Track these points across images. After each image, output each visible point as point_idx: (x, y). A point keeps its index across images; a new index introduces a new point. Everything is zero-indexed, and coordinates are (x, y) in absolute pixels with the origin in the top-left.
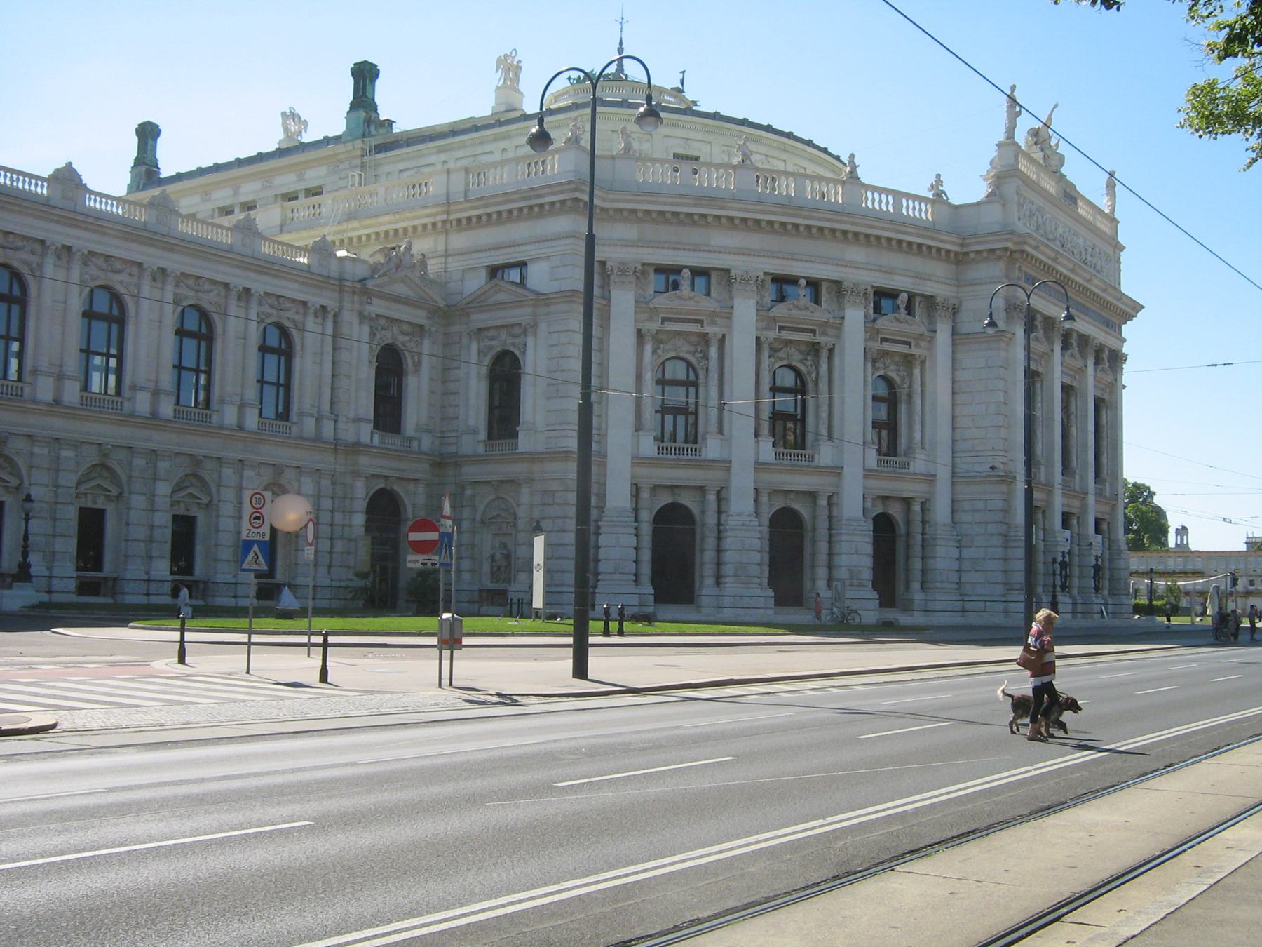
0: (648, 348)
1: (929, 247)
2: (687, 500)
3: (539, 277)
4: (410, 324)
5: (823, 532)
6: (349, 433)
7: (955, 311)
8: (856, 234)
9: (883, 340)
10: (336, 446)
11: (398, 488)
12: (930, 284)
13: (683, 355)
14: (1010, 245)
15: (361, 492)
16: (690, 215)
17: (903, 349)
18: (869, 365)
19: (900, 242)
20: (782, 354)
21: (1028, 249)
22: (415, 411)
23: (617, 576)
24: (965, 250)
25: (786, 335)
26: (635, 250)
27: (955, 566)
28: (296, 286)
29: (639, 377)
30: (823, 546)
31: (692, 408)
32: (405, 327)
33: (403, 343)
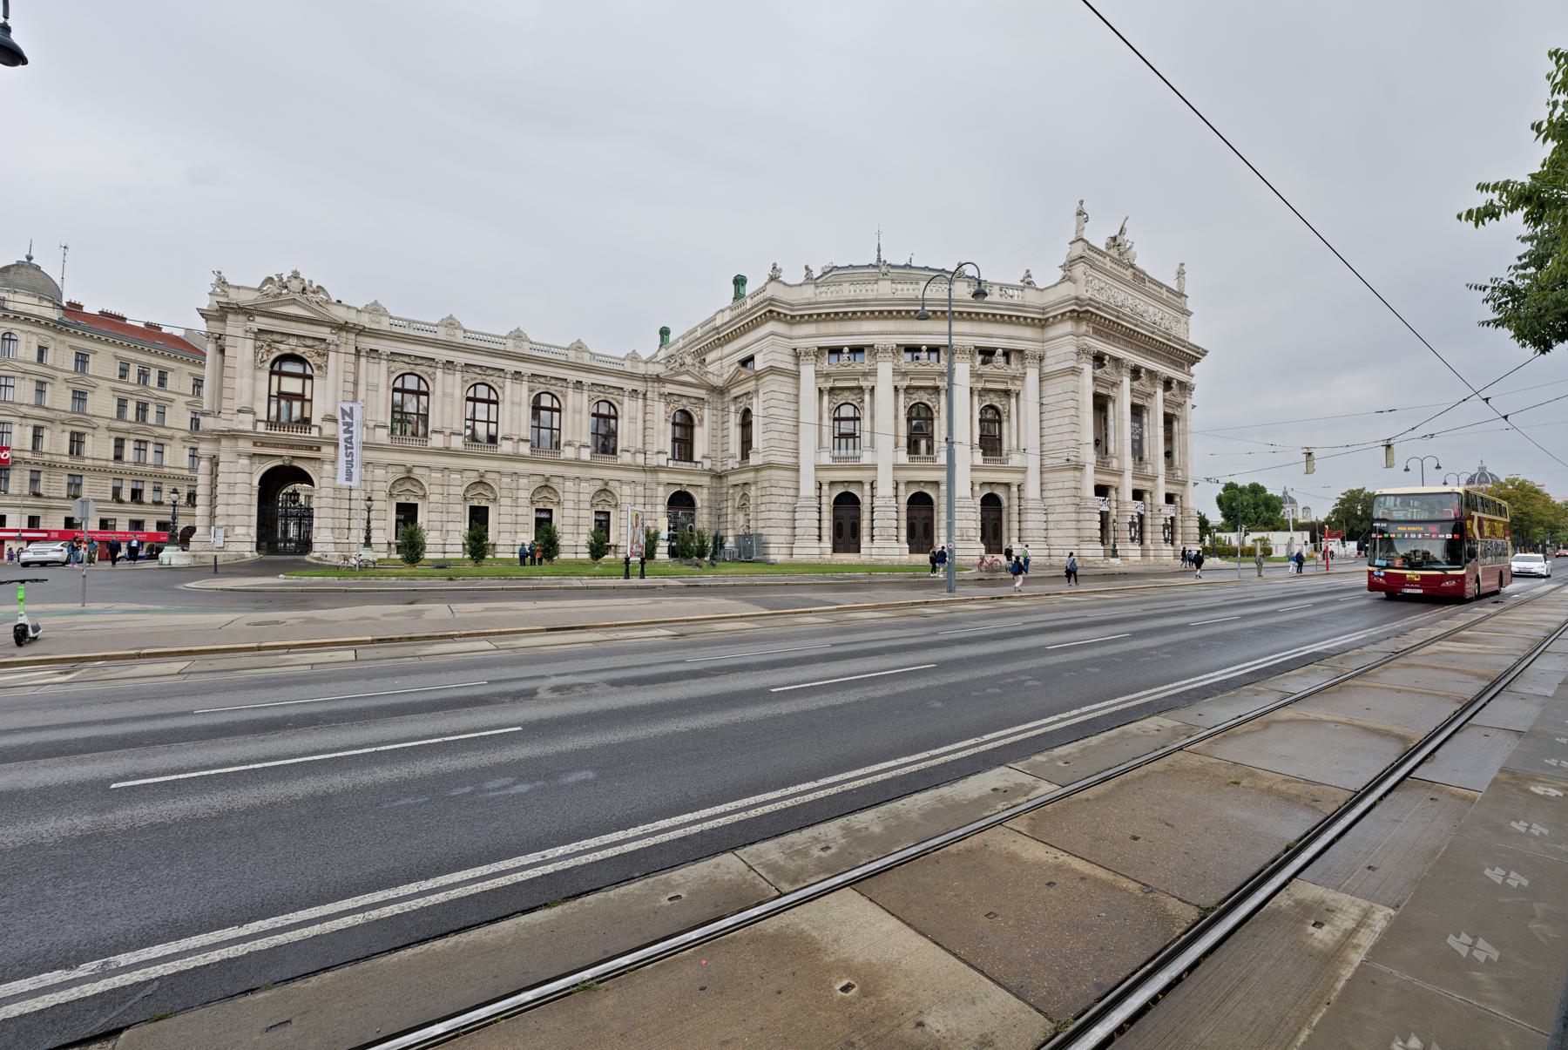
0: (826, 398)
2: (853, 490)
5: (943, 507)
6: (654, 461)
10: (644, 469)
11: (690, 490)
15: (663, 495)
18: (976, 398)
22: (700, 447)
30: (943, 516)
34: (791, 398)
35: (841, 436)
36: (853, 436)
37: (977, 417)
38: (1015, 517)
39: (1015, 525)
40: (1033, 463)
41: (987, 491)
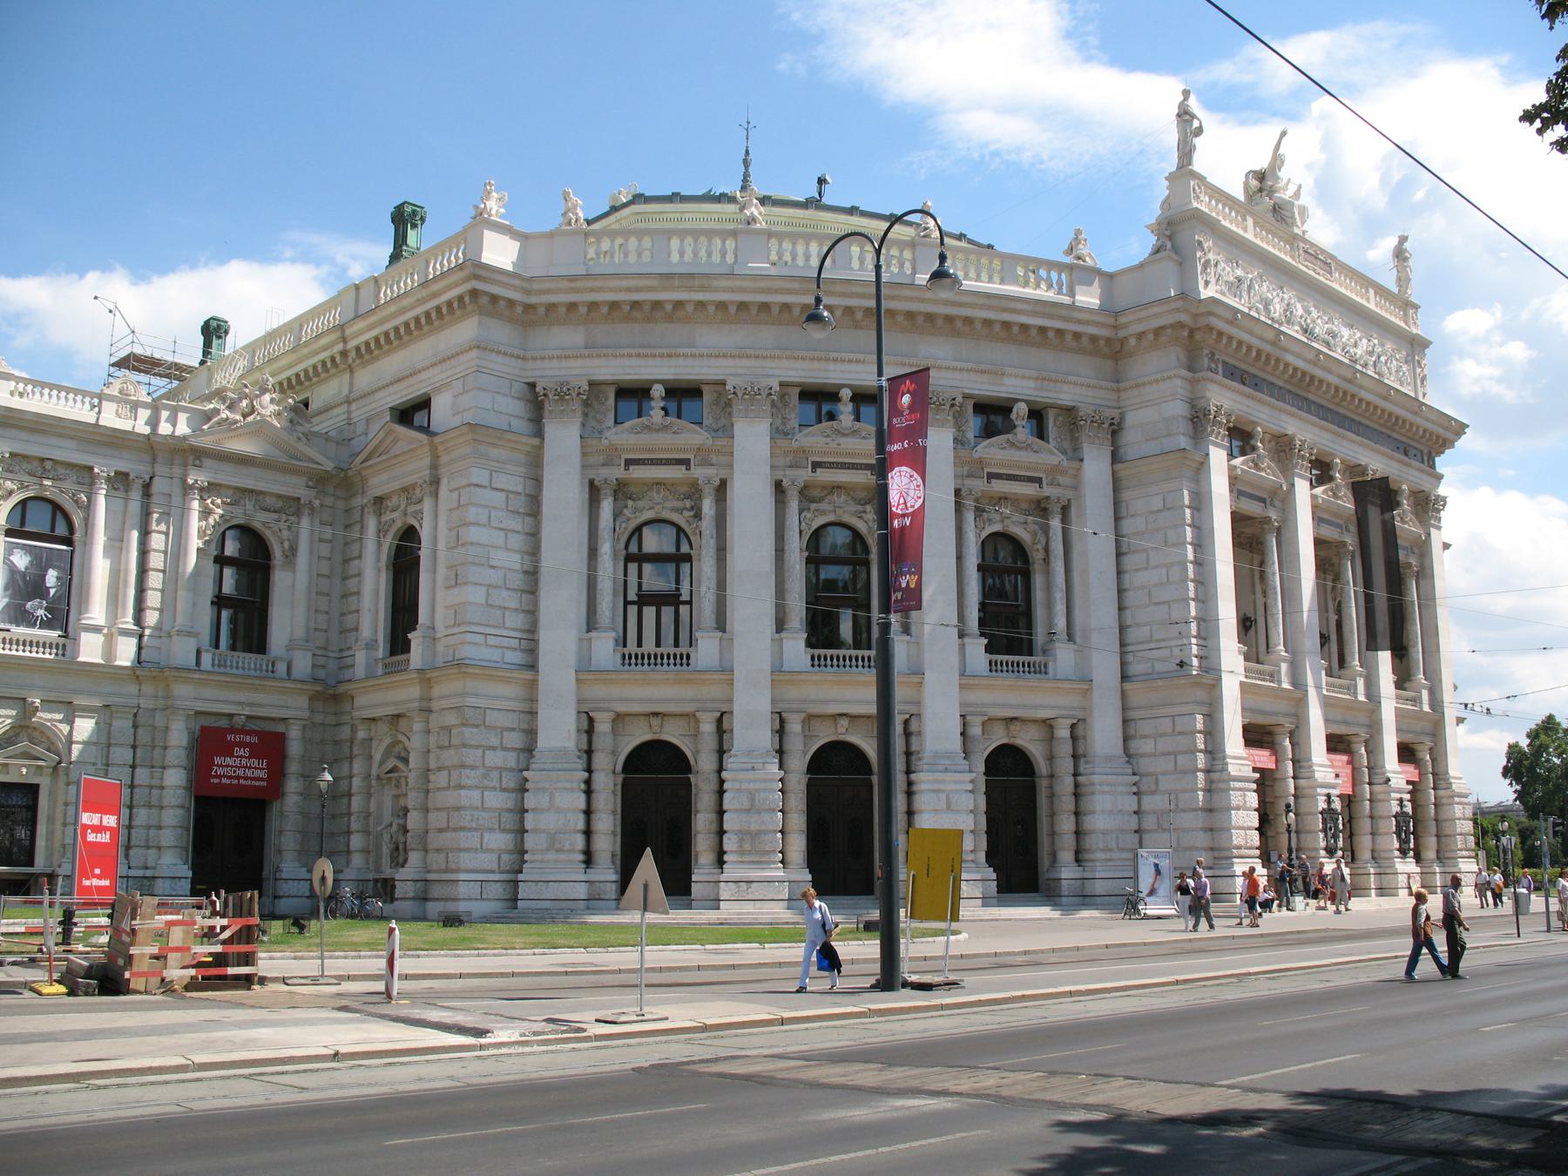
0: (607, 506)
1: (1060, 332)
2: (672, 734)
3: (442, 411)
4: (279, 496)
7: (1115, 430)
8: (930, 317)
9: (991, 476)
12: (1066, 387)
13: (666, 515)
14: (1184, 318)
16: (657, 305)
17: (1029, 490)
18: (970, 517)
19: (1006, 325)
20: (824, 506)
21: (1214, 322)
23: (551, 856)
24: (1121, 334)
25: (824, 476)
26: (579, 362)
27: (1133, 823)
28: (73, 444)
29: (593, 552)
31: (685, 597)
32: (269, 501)
33: (264, 523)
34: (520, 504)
35: (644, 599)
36: (673, 599)
37: (972, 560)
38: (1066, 803)
39: (1066, 824)
40: (1105, 668)
41: (999, 738)
